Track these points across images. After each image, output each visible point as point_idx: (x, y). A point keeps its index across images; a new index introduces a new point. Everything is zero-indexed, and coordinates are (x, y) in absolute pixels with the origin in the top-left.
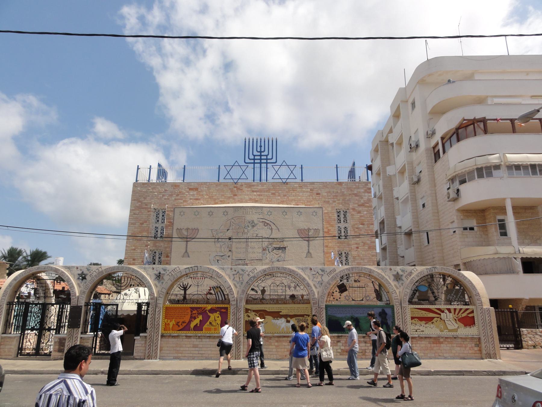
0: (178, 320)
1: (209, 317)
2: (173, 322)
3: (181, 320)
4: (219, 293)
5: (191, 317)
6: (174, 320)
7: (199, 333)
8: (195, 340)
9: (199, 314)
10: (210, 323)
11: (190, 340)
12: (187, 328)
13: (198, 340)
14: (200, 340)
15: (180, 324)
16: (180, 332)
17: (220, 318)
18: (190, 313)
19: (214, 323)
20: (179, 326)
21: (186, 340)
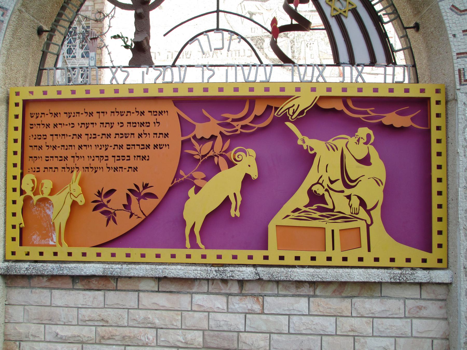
0: (104, 181)
1: (308, 158)
2: (74, 190)
3: (123, 182)
4: (350, 23)
5: (186, 159)
6: (76, 176)
7: (243, 264)
8: (219, 302)
9: (236, 138)
10: (315, 198)
11: (183, 301)
12: (156, 222)
13: (238, 304)
14: (249, 304)
15: (116, 202)
16: (121, 252)
17: (378, 168)
18: (176, 139)
19: (340, 203)
20: (110, 216)
21: (162, 300)
